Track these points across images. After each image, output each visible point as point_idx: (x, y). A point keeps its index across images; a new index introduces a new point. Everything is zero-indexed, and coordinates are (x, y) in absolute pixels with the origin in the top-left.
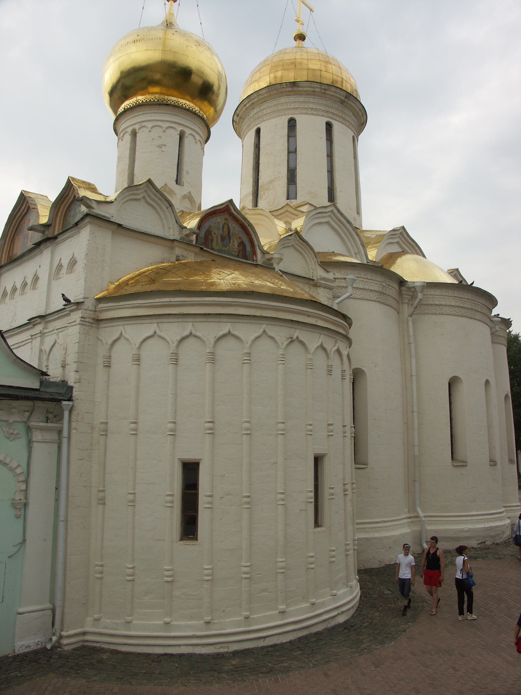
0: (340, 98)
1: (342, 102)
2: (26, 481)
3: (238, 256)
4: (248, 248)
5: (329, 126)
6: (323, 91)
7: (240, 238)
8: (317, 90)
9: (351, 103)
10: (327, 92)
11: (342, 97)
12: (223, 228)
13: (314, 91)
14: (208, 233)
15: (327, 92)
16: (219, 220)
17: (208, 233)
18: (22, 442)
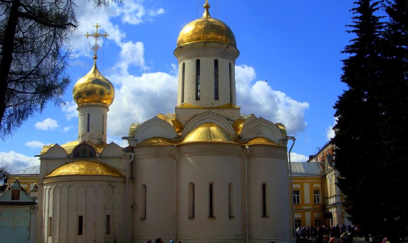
0: (201, 46)
1: (204, 46)
2: (30, 223)
3: (89, 157)
4: (93, 153)
5: (198, 62)
6: (192, 46)
7: (90, 151)
8: (190, 47)
9: (209, 45)
10: (194, 46)
11: (203, 45)
12: (83, 149)
13: (189, 48)
14: (78, 153)
15: (194, 46)
16: (82, 147)
17: (78, 153)
18: (29, 214)
